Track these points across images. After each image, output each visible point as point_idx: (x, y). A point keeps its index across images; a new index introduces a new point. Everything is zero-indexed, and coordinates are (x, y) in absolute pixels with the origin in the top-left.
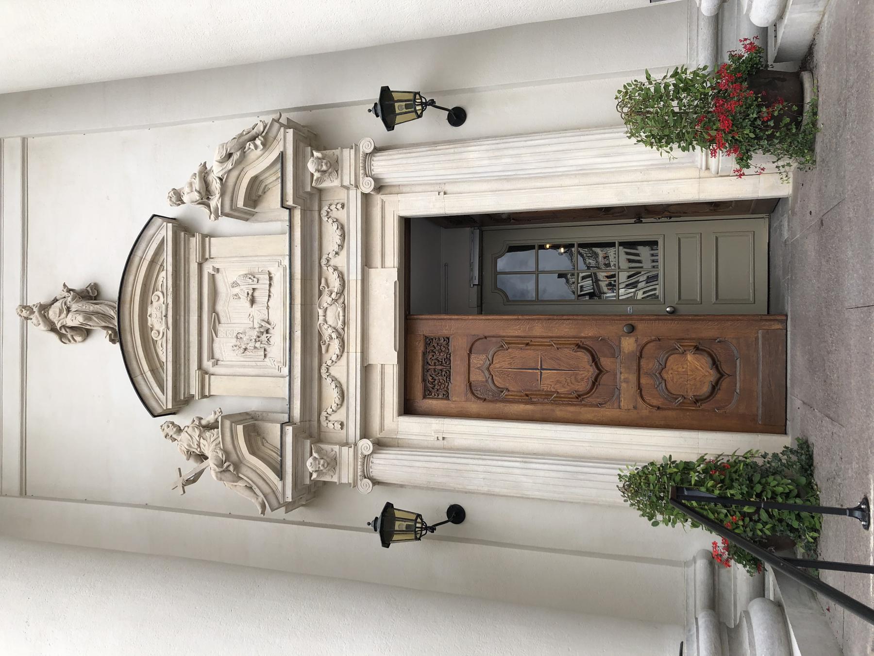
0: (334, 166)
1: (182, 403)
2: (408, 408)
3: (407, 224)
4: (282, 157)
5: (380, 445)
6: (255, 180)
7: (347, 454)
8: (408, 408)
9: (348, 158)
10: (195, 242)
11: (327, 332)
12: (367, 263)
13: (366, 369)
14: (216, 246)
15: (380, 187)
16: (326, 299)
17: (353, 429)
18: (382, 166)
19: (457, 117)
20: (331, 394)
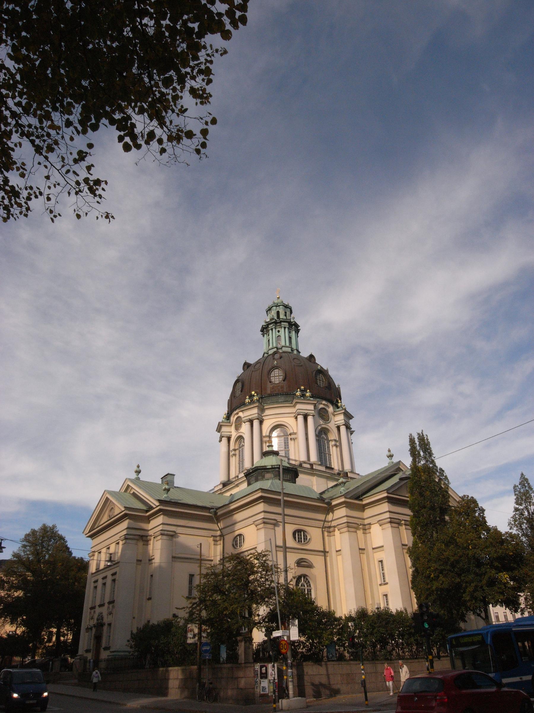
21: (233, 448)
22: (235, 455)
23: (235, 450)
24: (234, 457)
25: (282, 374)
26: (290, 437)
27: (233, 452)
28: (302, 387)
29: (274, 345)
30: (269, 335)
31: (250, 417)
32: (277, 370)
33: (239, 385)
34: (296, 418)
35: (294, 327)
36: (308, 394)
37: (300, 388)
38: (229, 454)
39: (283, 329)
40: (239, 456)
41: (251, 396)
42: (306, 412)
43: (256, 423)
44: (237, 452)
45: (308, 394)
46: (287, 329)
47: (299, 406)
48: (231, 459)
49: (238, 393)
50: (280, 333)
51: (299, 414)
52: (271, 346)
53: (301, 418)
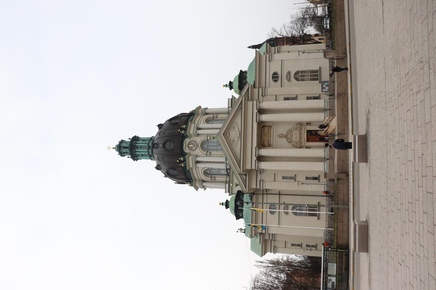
0: (303, 127)
1: (291, 142)
2: (307, 142)
3: (307, 130)
4: (300, 126)
5: (306, 144)
6: (297, 127)
7: (303, 144)
8: (307, 142)
9: (304, 126)
10: (292, 131)
11: (302, 137)
12: (304, 133)
13: (304, 139)
14: (293, 131)
15: (306, 128)
16: (302, 135)
17: (304, 143)
18: (306, 127)
19: (310, 124)
20: (302, 141)
21: (210, 178)
22: (215, 177)
23: (211, 177)
24: (216, 178)
25: (169, 142)
26: (209, 140)
27: (213, 179)
28: (179, 130)
29: (147, 151)
30: (139, 155)
31: (194, 163)
32: (166, 145)
33: (171, 172)
34: (198, 135)
35: (135, 139)
36: (184, 126)
37: (180, 131)
38: (213, 182)
39: (137, 144)
40: (215, 174)
41: (181, 162)
42: (195, 128)
43: (199, 159)
44: (213, 176)
45: (184, 126)
46: (137, 142)
47: (191, 132)
48: (217, 180)
49: (175, 172)
50: (139, 147)
51: (196, 132)
52: (147, 153)
53: (200, 132)
